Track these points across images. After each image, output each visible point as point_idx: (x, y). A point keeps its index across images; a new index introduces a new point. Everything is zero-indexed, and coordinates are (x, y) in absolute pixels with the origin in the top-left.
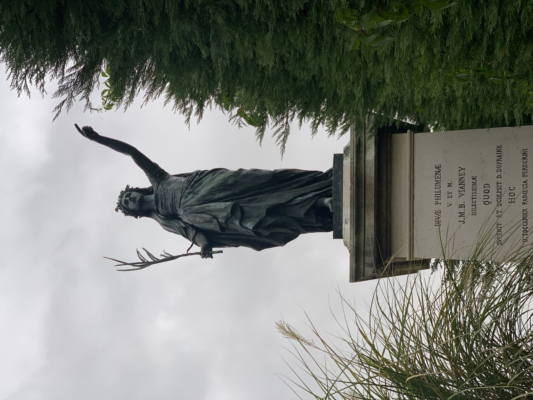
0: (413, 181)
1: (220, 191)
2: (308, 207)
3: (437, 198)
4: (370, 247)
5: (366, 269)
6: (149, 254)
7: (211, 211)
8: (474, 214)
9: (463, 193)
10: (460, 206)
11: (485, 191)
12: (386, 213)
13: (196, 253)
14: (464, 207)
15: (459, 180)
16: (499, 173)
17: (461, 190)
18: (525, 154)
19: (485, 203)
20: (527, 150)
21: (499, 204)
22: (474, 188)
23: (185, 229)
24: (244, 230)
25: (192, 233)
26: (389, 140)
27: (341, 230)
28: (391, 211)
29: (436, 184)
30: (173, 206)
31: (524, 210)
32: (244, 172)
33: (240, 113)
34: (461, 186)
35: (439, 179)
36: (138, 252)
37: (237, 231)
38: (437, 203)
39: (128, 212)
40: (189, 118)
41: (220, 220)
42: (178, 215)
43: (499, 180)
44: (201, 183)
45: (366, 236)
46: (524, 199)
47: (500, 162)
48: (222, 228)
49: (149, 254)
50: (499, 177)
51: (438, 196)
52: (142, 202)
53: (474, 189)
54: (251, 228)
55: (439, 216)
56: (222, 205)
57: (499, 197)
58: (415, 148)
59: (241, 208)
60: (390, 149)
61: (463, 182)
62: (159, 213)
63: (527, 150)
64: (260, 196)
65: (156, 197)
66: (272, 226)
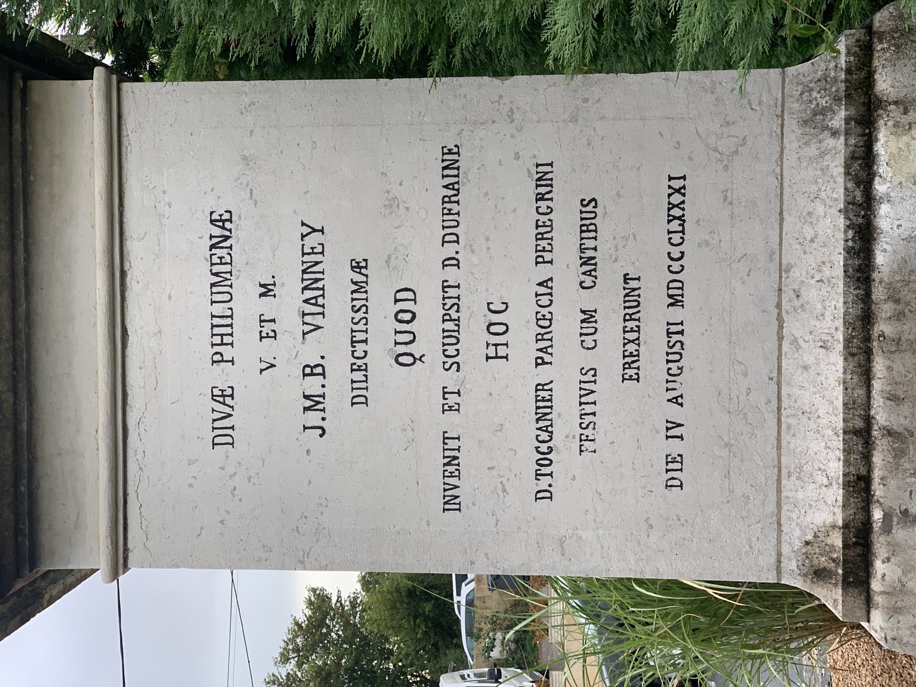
0: (123, 274)
3: (217, 340)
8: (360, 399)
9: (318, 320)
10: (308, 370)
11: (400, 316)
12: (12, 400)
14: (323, 374)
15: (304, 272)
16: (449, 251)
17: (309, 309)
18: (543, 180)
19: (401, 359)
20: (551, 165)
21: (452, 363)
22: (358, 304)
26: (17, 104)
29: (213, 285)
31: (539, 387)
34: (309, 294)
35: (227, 268)
38: (217, 358)
46: (542, 344)
47: (455, 208)
50: (451, 262)
53: (360, 309)
55: (228, 410)
57: (451, 337)
58: (125, 141)
60: (24, 143)
61: (317, 280)
63: (551, 165)
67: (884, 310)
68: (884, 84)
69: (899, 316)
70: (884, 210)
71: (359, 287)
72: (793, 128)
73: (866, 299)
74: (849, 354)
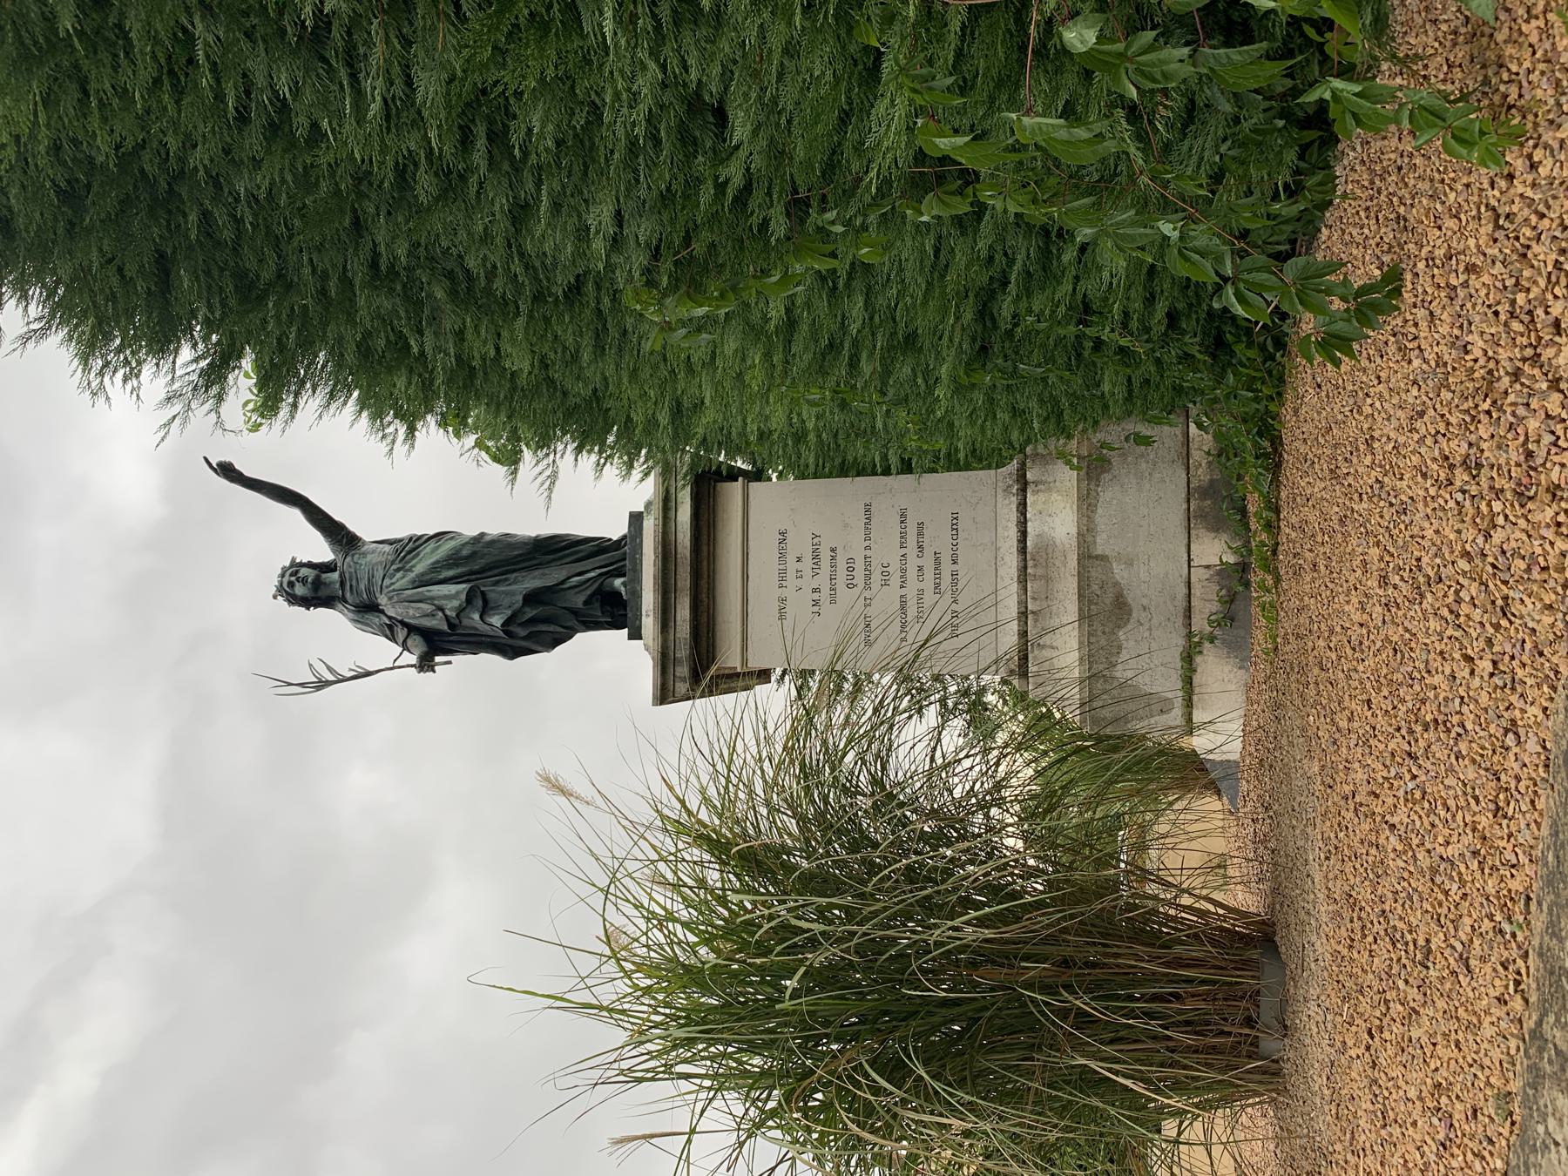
1: (449, 566)
2: (589, 592)
4: (683, 652)
5: (677, 685)
6: (329, 669)
7: (433, 598)
8: (833, 602)
13: (408, 666)
16: (867, 543)
21: (868, 586)
23: (390, 627)
24: (488, 628)
25: (401, 633)
27: (640, 627)
28: (714, 597)
30: (369, 591)
31: (902, 597)
32: (488, 538)
33: (479, 444)
36: (311, 665)
37: (476, 629)
39: (294, 600)
40: (392, 449)
41: (448, 613)
42: (378, 605)
43: (868, 553)
44: (418, 554)
45: (678, 635)
48: (451, 625)
49: (329, 669)
50: (868, 548)
51: (783, 575)
52: (317, 584)
54: (499, 625)
56: (452, 589)
57: (868, 577)
59: (483, 593)
62: (346, 602)
64: (514, 575)
65: (342, 575)
66: (532, 621)
67: (1030, 563)
68: (1029, 476)
69: (1035, 566)
70: (1029, 524)
71: (833, 558)
72: (999, 491)
73: (1025, 560)
74: (1019, 582)
